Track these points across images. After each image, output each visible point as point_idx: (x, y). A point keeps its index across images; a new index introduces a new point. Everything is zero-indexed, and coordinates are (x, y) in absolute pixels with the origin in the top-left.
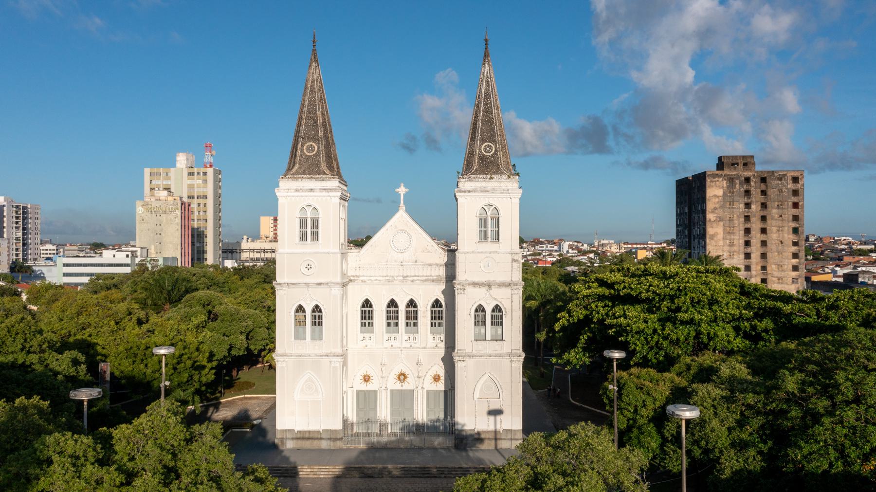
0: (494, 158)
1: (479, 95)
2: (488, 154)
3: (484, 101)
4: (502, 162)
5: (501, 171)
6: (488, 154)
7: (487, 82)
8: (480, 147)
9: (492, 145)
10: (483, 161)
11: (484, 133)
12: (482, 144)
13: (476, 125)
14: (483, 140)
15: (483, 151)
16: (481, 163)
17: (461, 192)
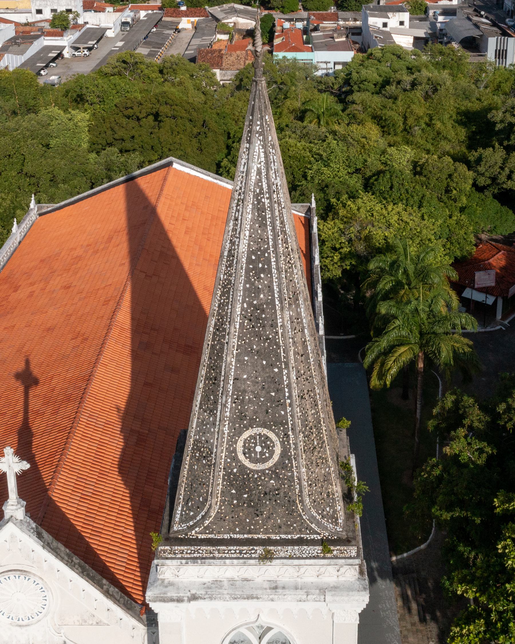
0: (277, 478)
1: (231, 254)
2: (260, 467)
3: (248, 280)
4: (306, 491)
5: (302, 523)
6: (260, 467)
7: (259, 208)
8: (232, 442)
9: (272, 435)
10: (240, 490)
11: (244, 391)
12: (240, 434)
13: (221, 358)
14: (242, 416)
15: (241, 457)
16: (232, 496)
17: (164, 600)
